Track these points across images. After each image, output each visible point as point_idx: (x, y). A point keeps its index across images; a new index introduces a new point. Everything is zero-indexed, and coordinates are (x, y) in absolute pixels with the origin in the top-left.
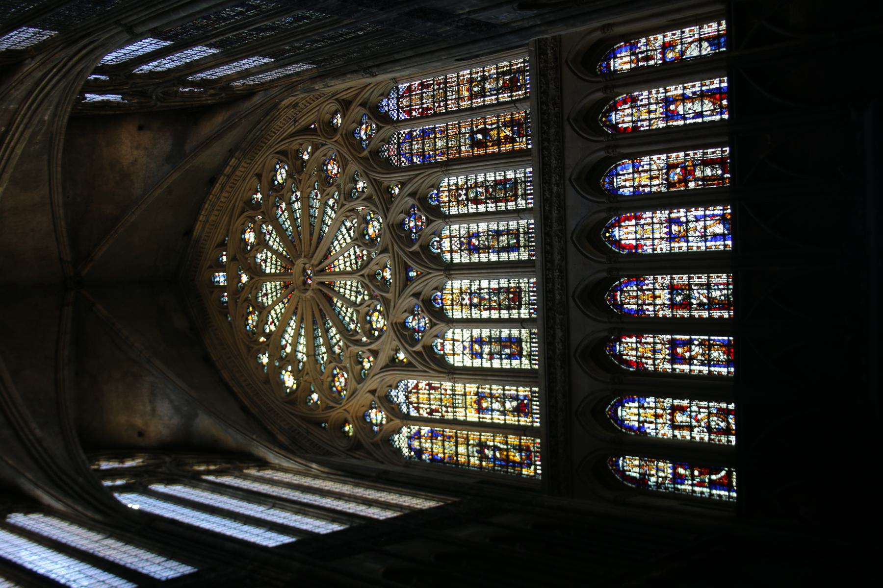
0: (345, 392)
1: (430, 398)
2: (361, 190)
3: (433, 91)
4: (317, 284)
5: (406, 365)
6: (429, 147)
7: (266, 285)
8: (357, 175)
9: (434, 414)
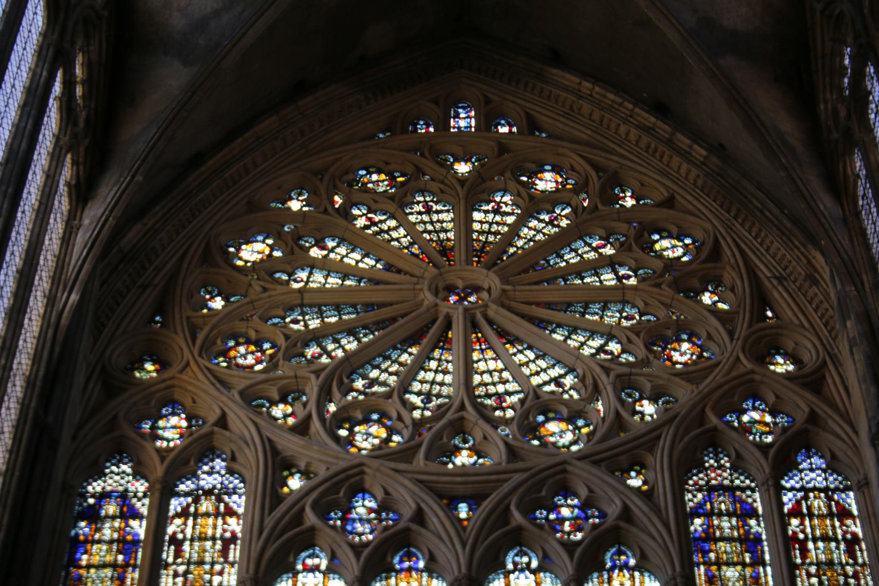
0: (225, 364)
2: (638, 408)
3: (840, 563)
4: (448, 313)
5: (277, 492)
6: (725, 552)
7: (448, 211)
8: (667, 402)
9: (172, 547)
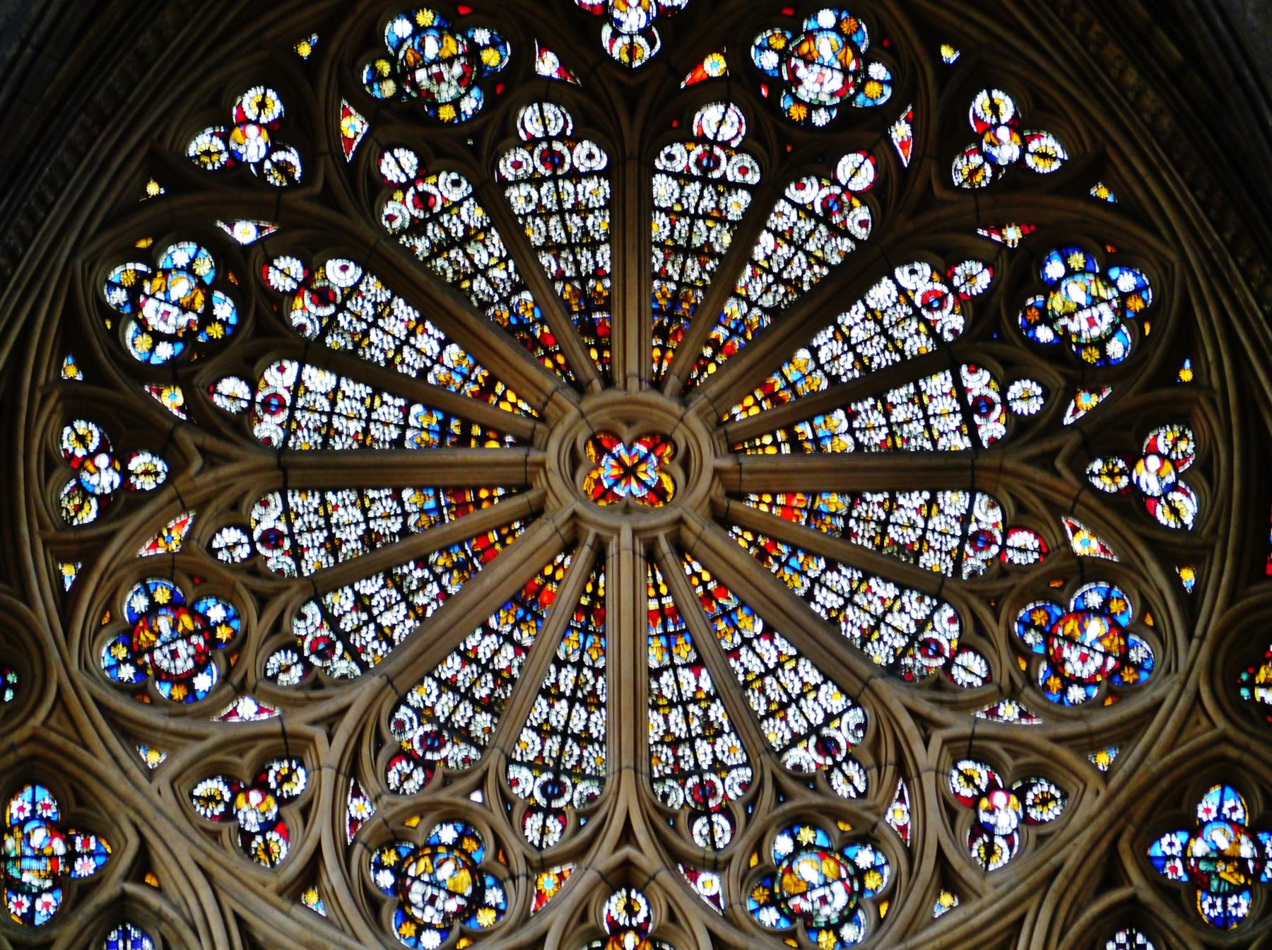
2: (984, 817)
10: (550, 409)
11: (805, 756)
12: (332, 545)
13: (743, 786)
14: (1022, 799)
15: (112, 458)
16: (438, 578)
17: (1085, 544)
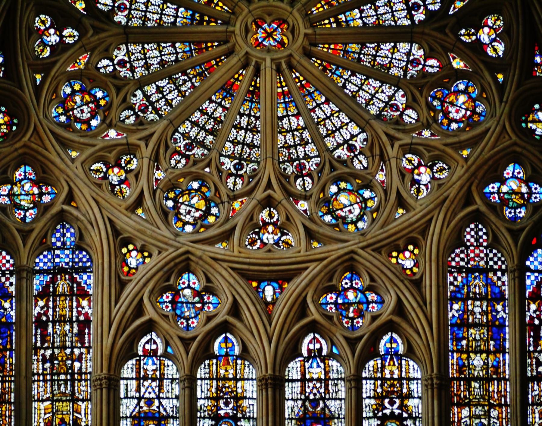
1: (65, 322)
2: (416, 177)
5: (119, 277)
6: (475, 339)
9: (39, 331)
10: (237, 9)
11: (343, 153)
12: (147, 66)
13: (317, 165)
14: (432, 169)
15: (56, 30)
16: (190, 79)
17: (458, 64)
